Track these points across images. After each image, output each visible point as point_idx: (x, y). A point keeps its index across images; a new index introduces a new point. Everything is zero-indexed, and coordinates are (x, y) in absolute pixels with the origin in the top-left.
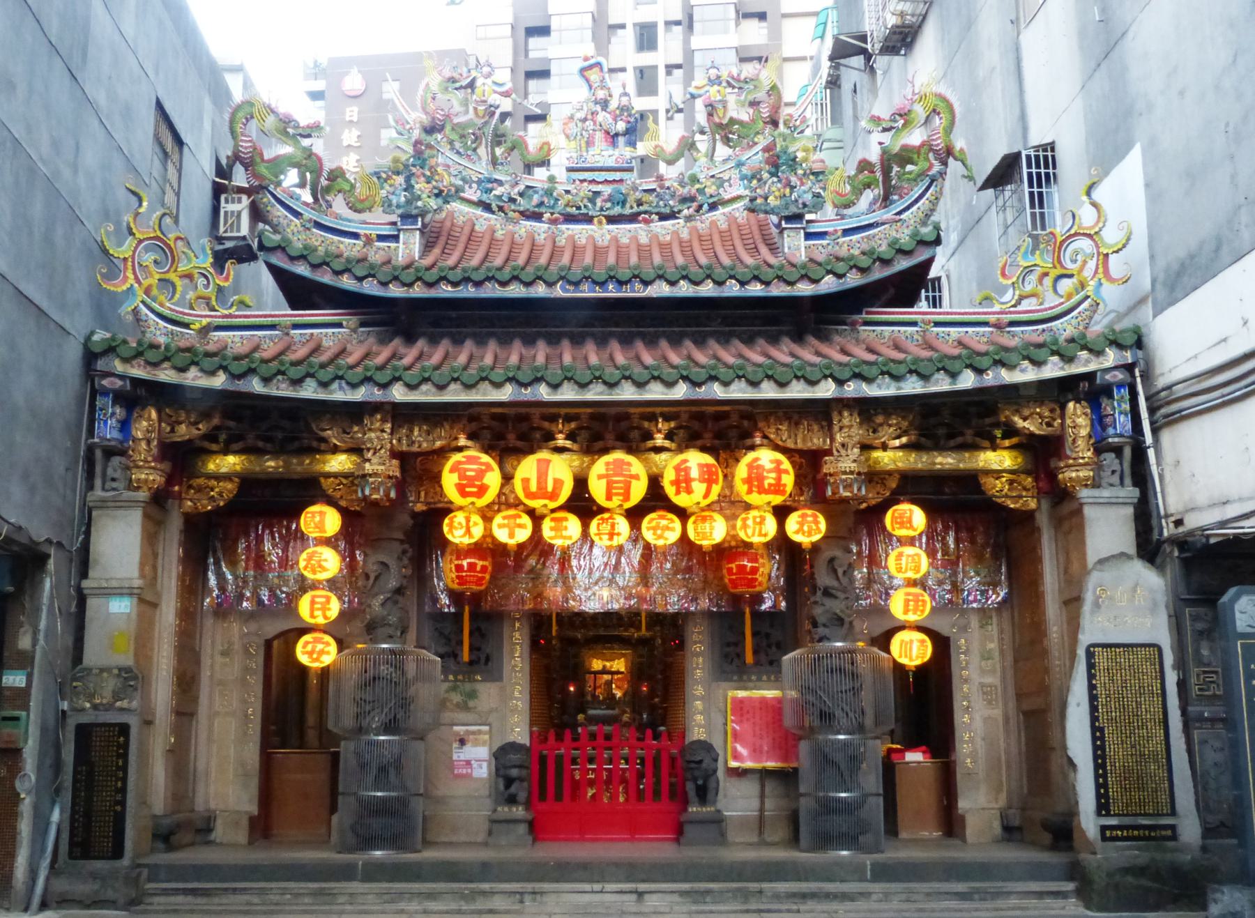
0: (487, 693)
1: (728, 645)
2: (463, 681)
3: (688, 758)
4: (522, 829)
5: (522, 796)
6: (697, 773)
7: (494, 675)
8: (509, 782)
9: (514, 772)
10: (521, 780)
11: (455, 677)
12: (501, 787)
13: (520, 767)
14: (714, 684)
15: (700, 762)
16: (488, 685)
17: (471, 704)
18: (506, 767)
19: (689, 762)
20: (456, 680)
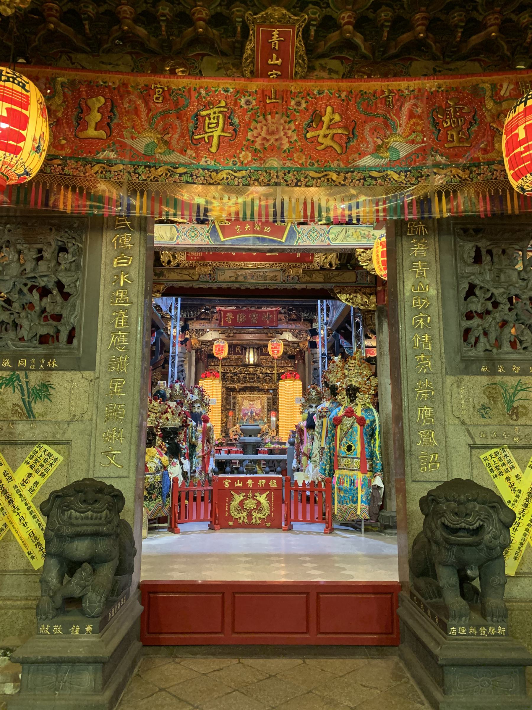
0: (70, 389)
1: (469, 316)
2: (27, 369)
3: (450, 520)
4: (87, 678)
5: (94, 601)
6: (468, 555)
7: (84, 363)
8: (70, 567)
9: (80, 548)
10: (95, 561)
11: (14, 362)
12: (53, 578)
13: (95, 535)
14: (450, 380)
15: (478, 531)
16: (69, 375)
17: (38, 407)
18: (60, 537)
19: (455, 531)
20: (15, 368)
